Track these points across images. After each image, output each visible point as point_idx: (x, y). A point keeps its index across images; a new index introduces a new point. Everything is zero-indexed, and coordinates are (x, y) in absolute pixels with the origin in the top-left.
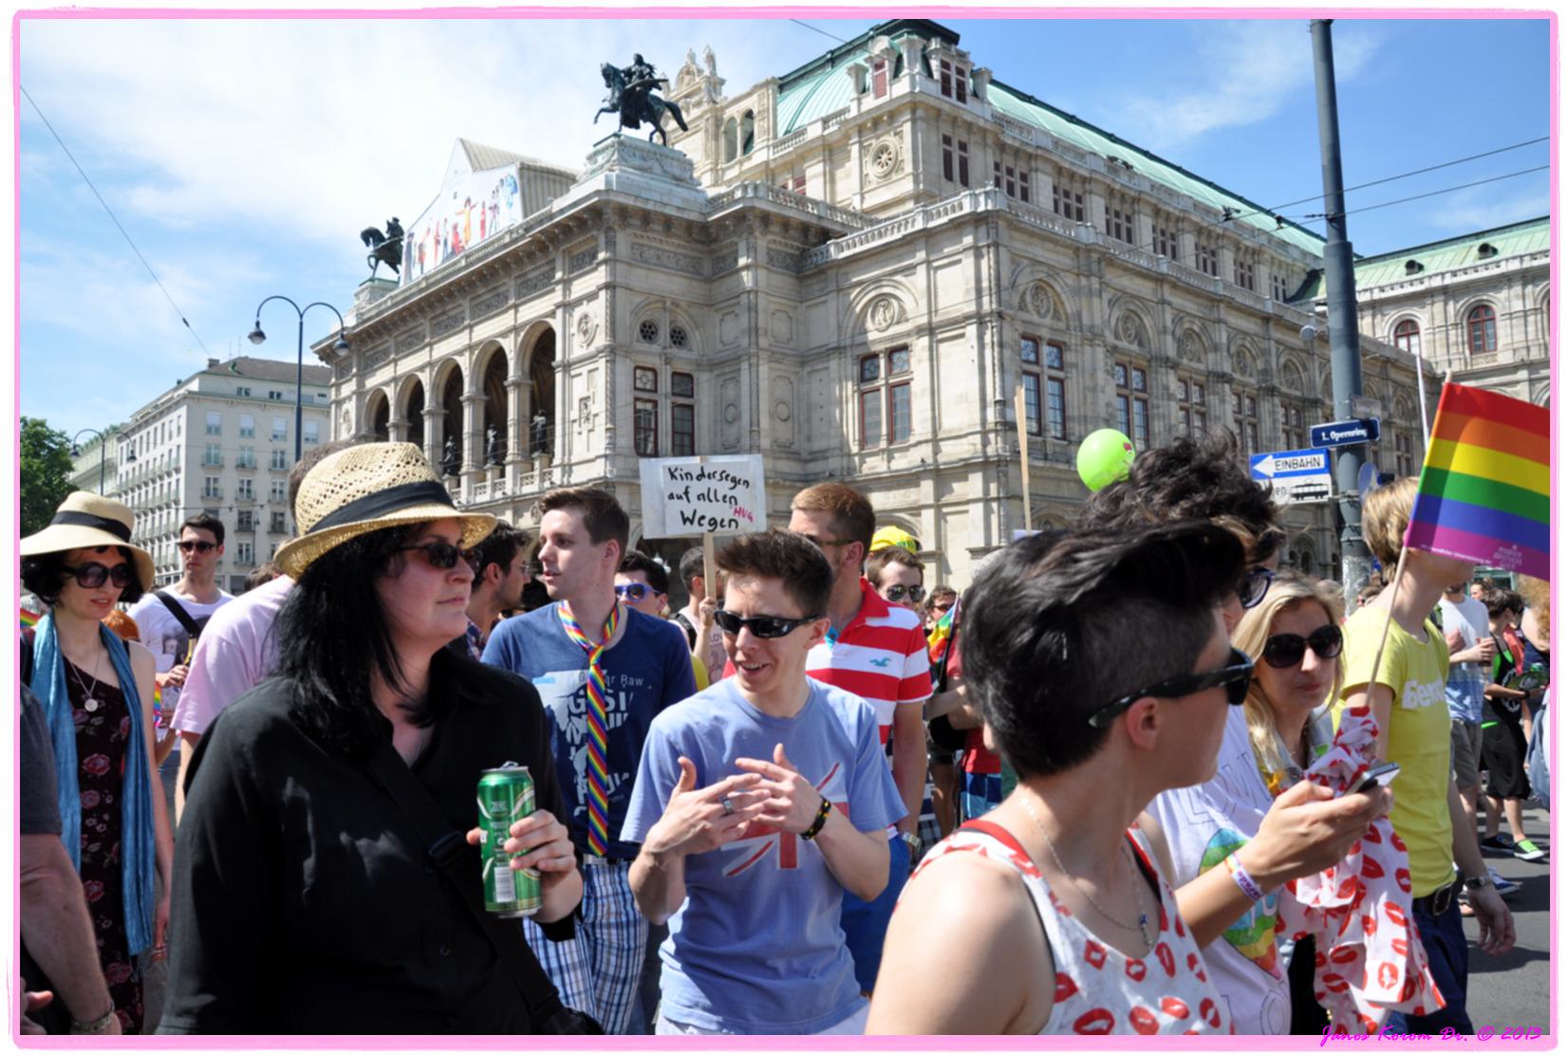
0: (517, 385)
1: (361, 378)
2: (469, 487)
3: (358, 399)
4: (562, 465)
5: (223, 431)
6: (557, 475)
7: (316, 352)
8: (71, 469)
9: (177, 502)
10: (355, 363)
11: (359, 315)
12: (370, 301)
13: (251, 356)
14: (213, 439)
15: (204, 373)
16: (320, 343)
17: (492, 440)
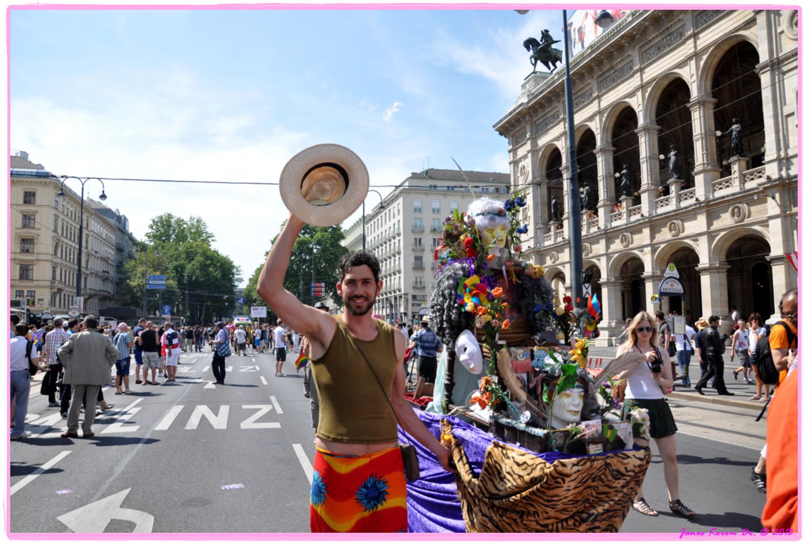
0: (701, 103)
1: (534, 139)
2: (650, 202)
3: (532, 156)
4: (779, 160)
5: (423, 210)
6: (771, 170)
7: (497, 130)
8: (343, 238)
9: (399, 253)
10: (528, 128)
11: (528, 96)
12: (535, 86)
13: (435, 168)
14: (418, 215)
15: (410, 178)
16: (501, 121)
17: (673, 158)
